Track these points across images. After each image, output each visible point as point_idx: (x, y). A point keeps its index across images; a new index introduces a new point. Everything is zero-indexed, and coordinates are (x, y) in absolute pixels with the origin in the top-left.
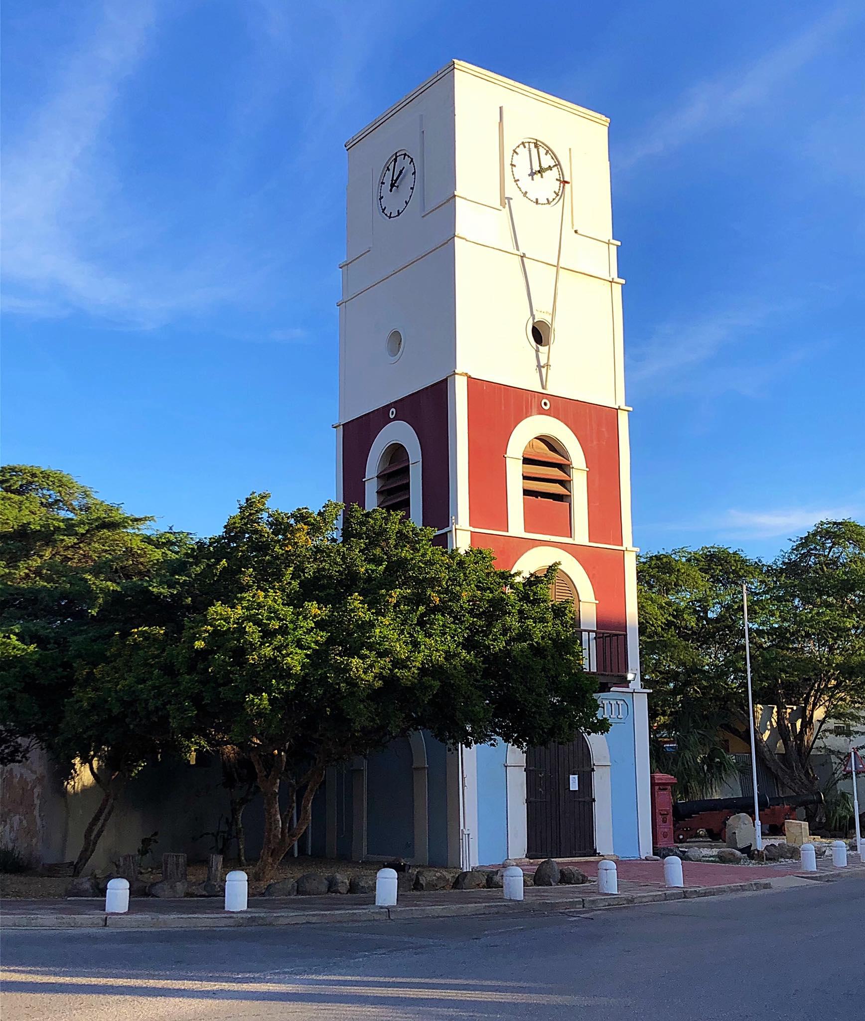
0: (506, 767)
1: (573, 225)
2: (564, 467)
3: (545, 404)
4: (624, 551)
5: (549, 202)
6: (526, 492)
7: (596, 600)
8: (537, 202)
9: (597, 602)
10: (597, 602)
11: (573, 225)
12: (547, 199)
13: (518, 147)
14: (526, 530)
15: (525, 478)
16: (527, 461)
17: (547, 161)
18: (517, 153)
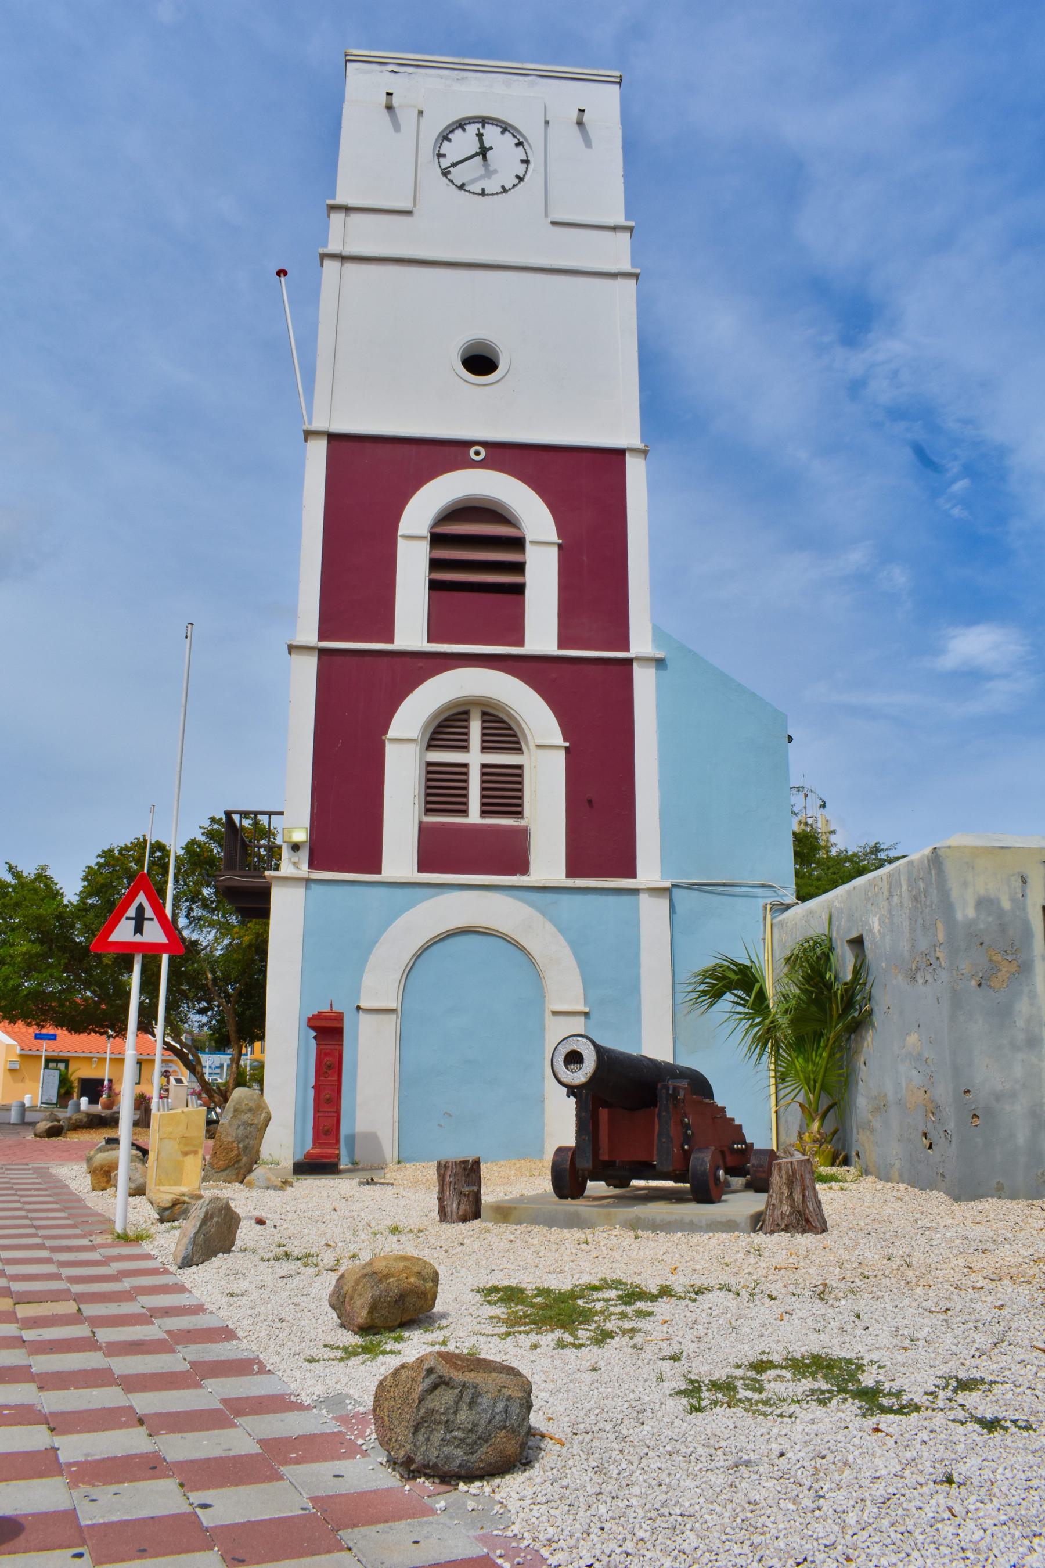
1: (546, 215)
2: (518, 543)
3: (477, 453)
4: (629, 662)
5: (505, 190)
6: (435, 586)
7: (565, 740)
8: (483, 193)
9: (567, 744)
10: (567, 744)
11: (546, 215)
12: (503, 187)
13: (452, 131)
14: (430, 641)
15: (435, 564)
16: (437, 540)
17: (491, 134)
18: (449, 140)
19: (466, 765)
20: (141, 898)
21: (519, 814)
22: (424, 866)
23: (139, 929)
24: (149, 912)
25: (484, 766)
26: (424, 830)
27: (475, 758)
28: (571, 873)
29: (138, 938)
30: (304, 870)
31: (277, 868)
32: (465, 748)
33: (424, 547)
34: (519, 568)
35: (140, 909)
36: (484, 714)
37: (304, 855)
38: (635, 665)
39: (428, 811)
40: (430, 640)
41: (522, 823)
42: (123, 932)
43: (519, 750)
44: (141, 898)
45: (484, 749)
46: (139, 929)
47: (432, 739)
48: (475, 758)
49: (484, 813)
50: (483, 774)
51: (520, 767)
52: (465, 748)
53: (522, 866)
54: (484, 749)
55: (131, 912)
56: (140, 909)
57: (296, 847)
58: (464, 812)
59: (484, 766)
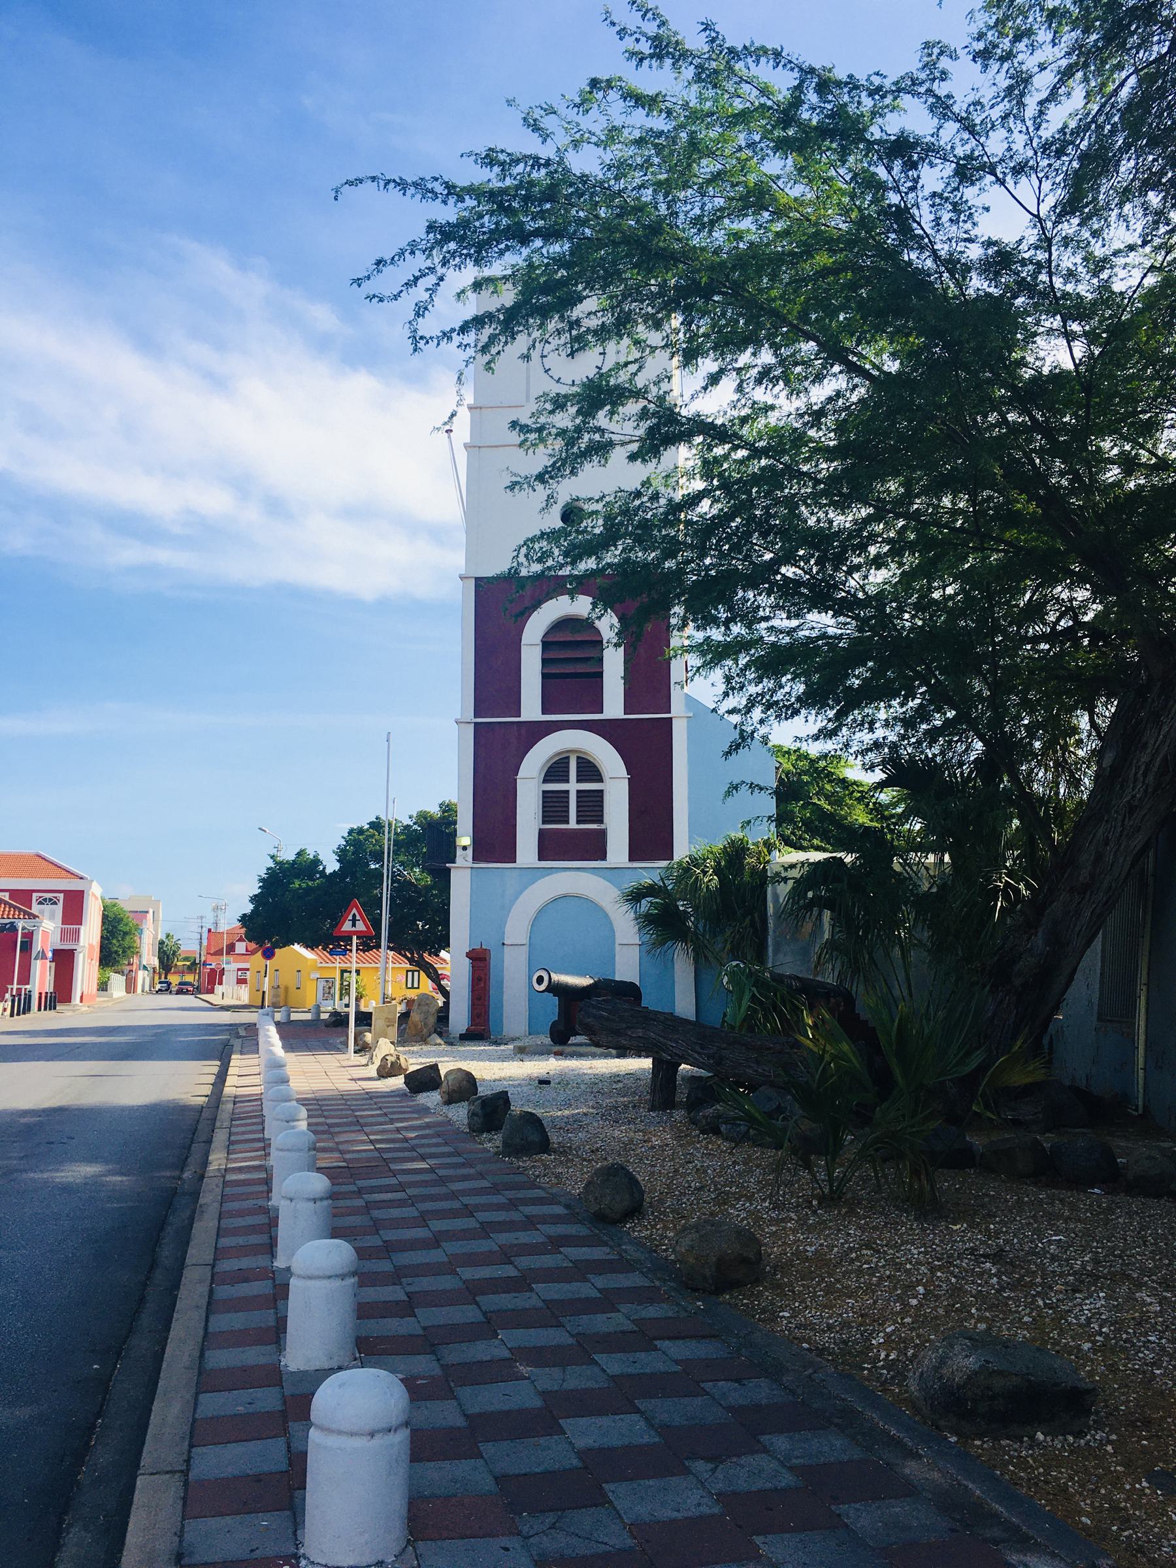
0: (503, 944)
6: (545, 676)
14: (543, 713)
15: (545, 662)
16: (546, 645)
19: (567, 792)
20: (354, 911)
21: (601, 822)
22: (541, 857)
23: (354, 925)
24: (358, 917)
25: (578, 792)
26: (542, 833)
27: (573, 786)
28: (631, 859)
29: (354, 929)
30: (470, 863)
31: (454, 862)
32: (567, 781)
33: (539, 649)
34: (601, 660)
35: (354, 915)
36: (578, 758)
37: (470, 851)
38: (674, 721)
39: (544, 822)
40: (543, 713)
41: (602, 826)
42: (347, 926)
43: (601, 780)
44: (354, 911)
45: (578, 781)
46: (354, 925)
47: (545, 776)
48: (573, 786)
49: (578, 822)
50: (578, 797)
51: (602, 791)
52: (567, 781)
53: (603, 856)
54: (578, 781)
55: (350, 917)
56: (354, 915)
57: (465, 848)
58: (567, 822)
59: (578, 792)
